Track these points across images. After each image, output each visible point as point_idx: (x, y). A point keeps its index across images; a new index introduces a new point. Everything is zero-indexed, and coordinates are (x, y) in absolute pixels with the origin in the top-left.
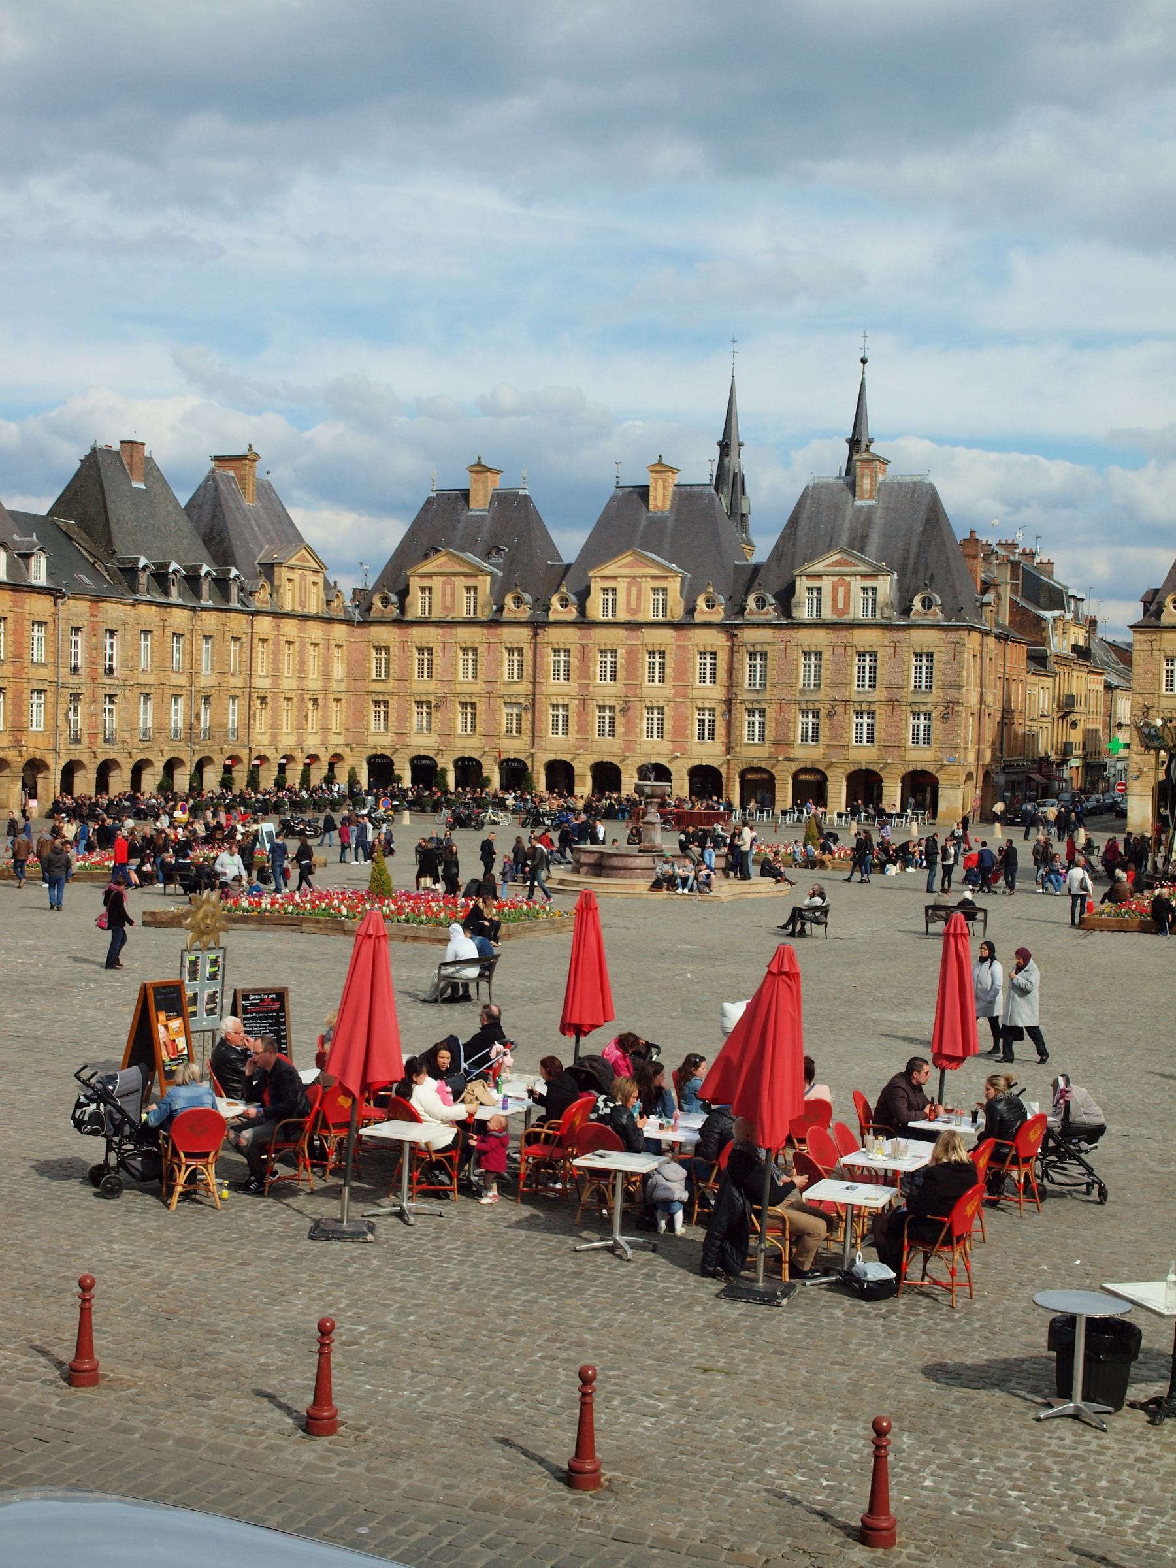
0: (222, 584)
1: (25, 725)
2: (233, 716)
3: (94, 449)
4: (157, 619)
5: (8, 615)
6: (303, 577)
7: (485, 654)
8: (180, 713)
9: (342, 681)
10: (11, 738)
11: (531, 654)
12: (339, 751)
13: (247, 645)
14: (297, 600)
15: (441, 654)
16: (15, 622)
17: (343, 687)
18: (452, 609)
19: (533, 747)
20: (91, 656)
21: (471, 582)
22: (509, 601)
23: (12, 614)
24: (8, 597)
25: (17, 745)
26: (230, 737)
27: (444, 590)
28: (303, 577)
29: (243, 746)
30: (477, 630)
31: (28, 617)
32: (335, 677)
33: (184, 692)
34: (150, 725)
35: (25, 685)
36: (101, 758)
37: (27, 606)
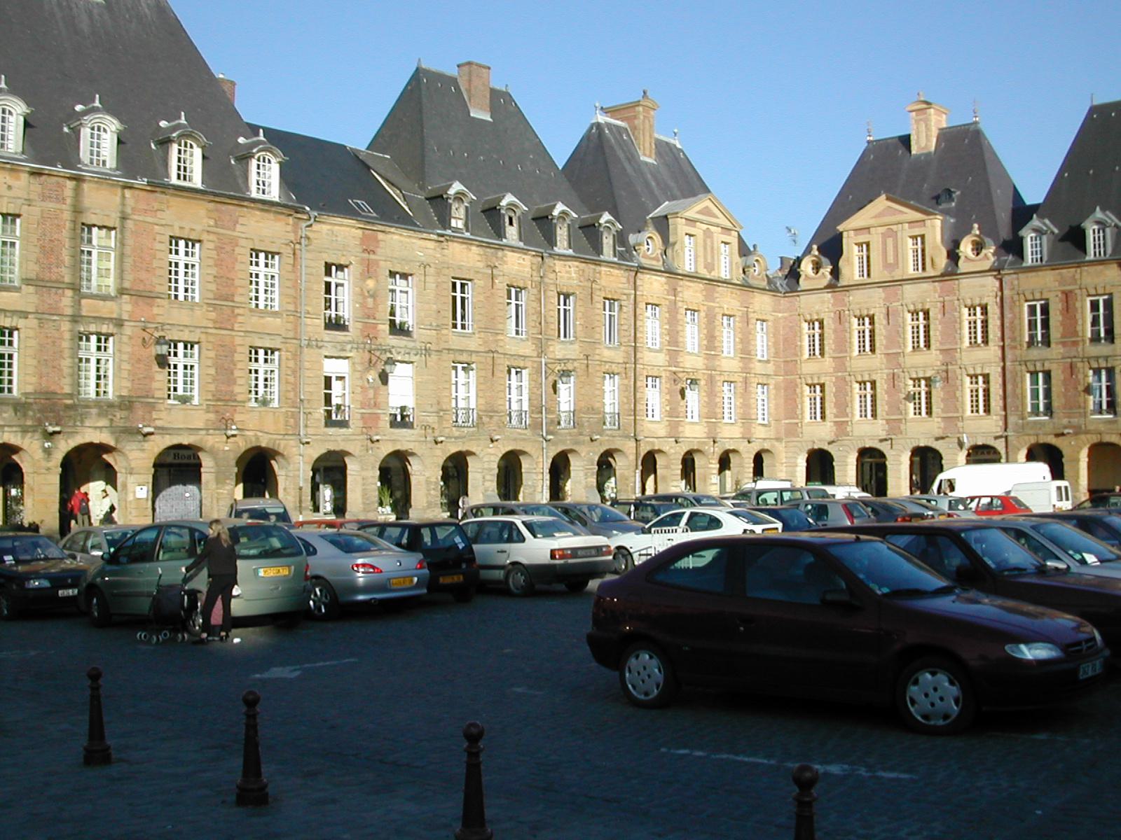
0: (589, 234)
1: (239, 398)
2: (611, 396)
3: (417, 69)
4: (481, 265)
5: (204, 237)
6: (708, 234)
7: (940, 316)
8: (525, 392)
9: (768, 362)
10: (212, 416)
11: (998, 311)
12: (766, 446)
13: (629, 308)
14: (701, 260)
15: (885, 322)
16: (219, 249)
17: (770, 368)
18: (896, 264)
19: (1006, 430)
20: (363, 305)
21: (917, 231)
22: (966, 248)
23: (212, 237)
24: (203, 212)
25: (224, 423)
26: (608, 426)
27: (884, 244)
28: (708, 234)
29: (627, 437)
30: (925, 286)
31: (242, 242)
32: (759, 357)
33: (529, 364)
34: (473, 405)
35: (238, 341)
36: (386, 449)
37: (239, 228)
